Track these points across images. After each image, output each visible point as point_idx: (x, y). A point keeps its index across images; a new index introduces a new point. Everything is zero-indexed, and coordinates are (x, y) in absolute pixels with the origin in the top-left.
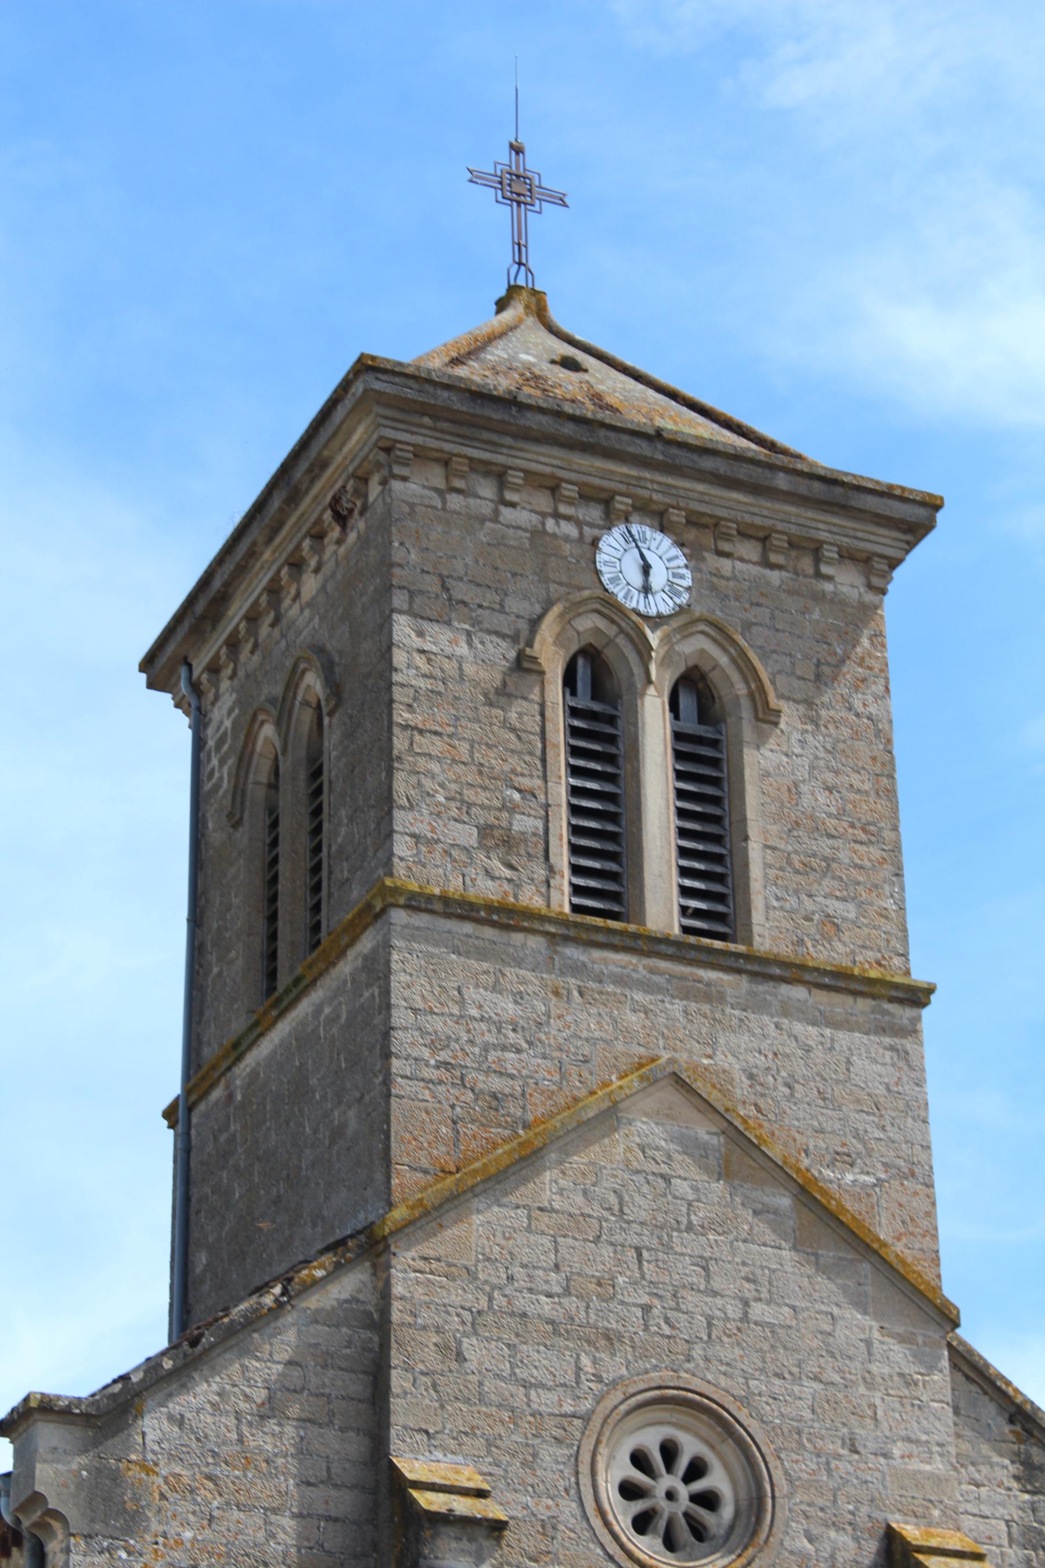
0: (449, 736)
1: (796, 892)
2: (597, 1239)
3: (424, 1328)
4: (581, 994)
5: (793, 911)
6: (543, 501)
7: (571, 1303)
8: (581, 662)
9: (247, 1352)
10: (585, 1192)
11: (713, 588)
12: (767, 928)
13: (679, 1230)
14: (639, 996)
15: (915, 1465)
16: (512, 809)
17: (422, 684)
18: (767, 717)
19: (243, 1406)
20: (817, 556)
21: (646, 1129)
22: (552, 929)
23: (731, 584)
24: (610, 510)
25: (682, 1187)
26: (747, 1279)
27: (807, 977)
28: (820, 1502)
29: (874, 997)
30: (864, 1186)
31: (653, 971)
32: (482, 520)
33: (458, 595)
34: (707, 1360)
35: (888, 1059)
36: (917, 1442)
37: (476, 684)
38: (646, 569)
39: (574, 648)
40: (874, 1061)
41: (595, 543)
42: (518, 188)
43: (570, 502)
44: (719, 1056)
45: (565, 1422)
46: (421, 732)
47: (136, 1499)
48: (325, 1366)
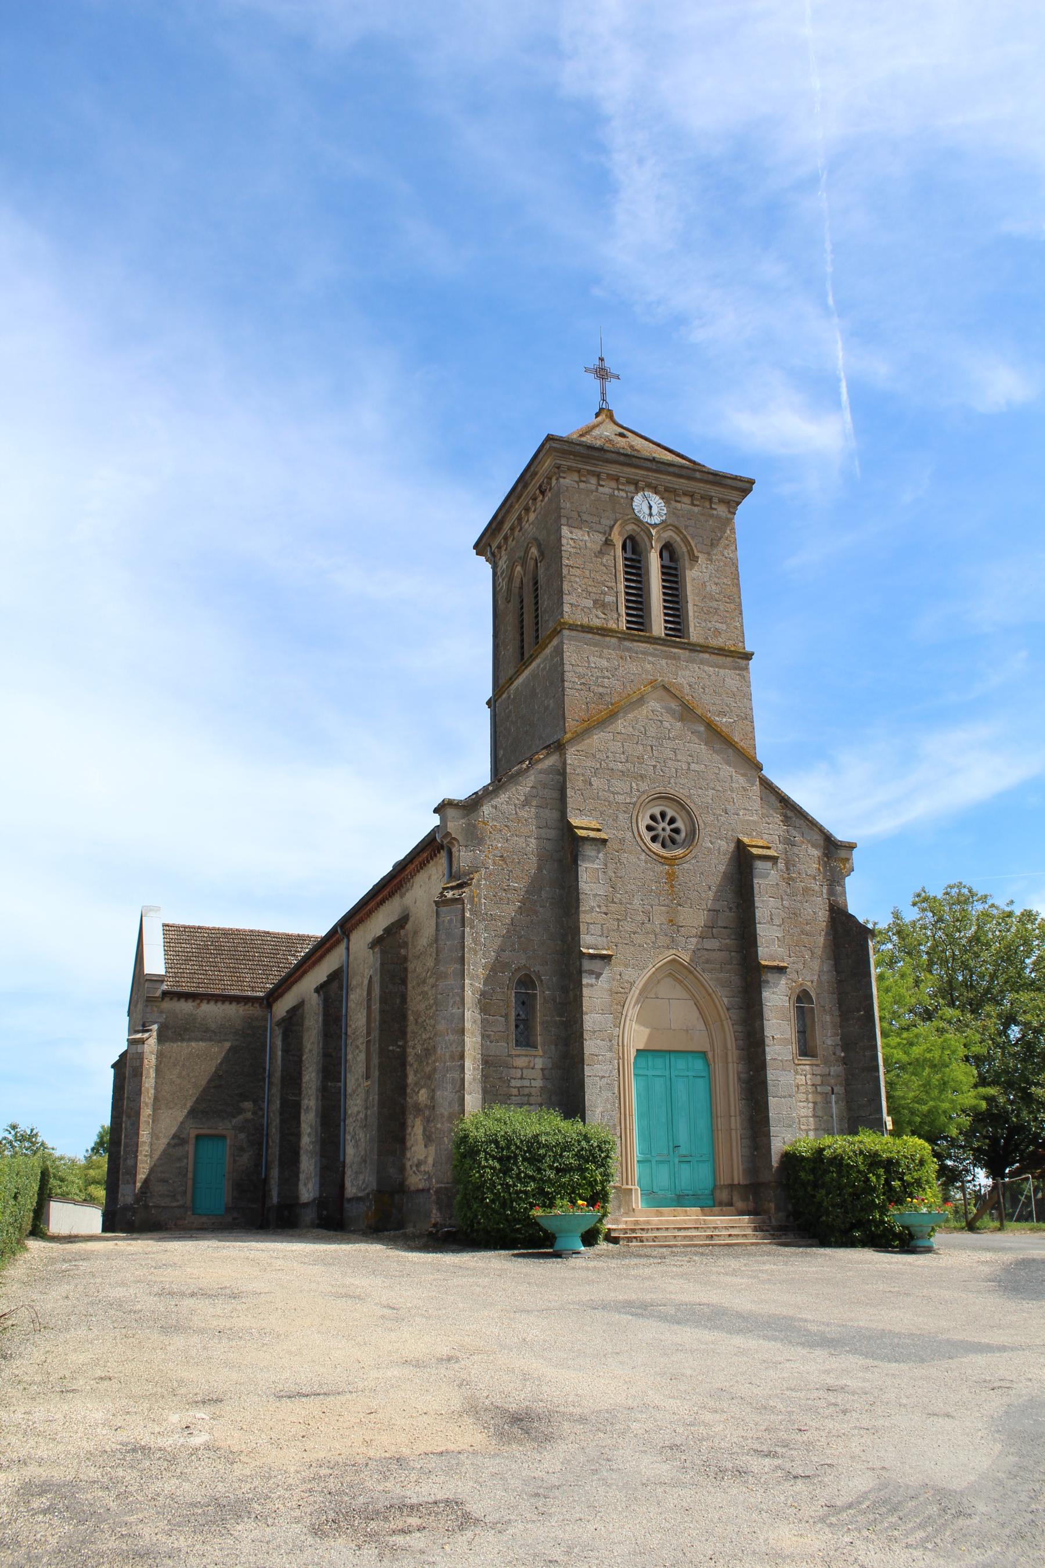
6: (614, 484)
7: (629, 765)
11: (674, 514)
12: (695, 634)
15: (747, 818)
17: (572, 550)
18: (694, 559)
20: (711, 502)
21: (653, 704)
24: (637, 486)
31: (656, 649)
32: (592, 492)
38: (650, 507)
42: (602, 373)
43: (623, 484)
47: (482, 833)
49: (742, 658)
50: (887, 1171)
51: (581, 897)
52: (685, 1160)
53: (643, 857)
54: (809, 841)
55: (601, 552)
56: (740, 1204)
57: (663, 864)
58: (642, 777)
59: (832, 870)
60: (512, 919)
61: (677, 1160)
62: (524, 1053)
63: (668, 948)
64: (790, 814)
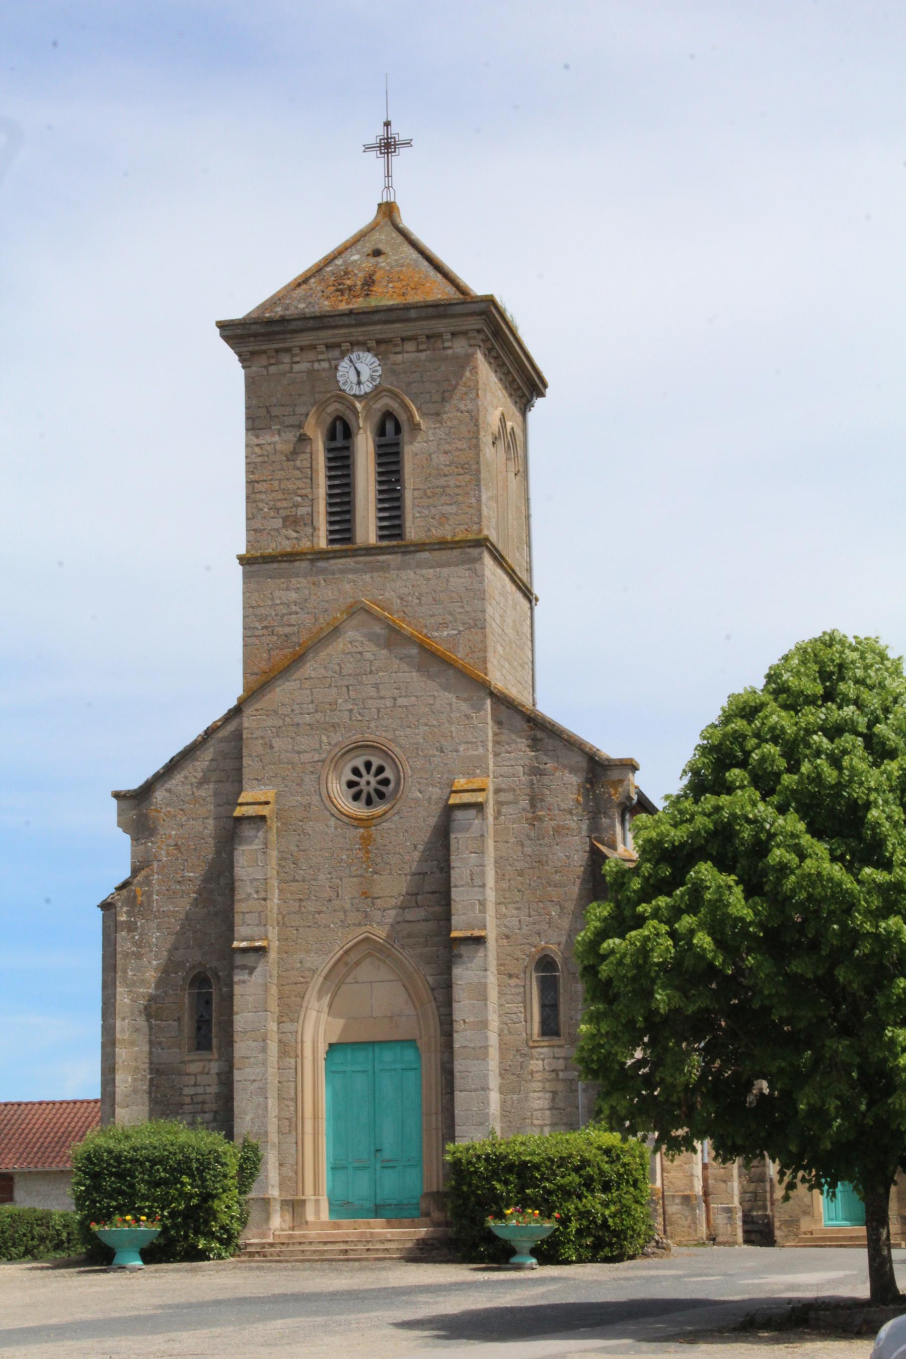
0: (271, 480)
1: (428, 507)
2: (330, 686)
3: (256, 738)
4: (325, 581)
5: (426, 516)
6: (311, 355)
7: (319, 716)
8: (338, 423)
9: (196, 760)
10: (325, 668)
11: (393, 372)
12: (413, 531)
13: (366, 674)
14: (350, 576)
15: (471, 752)
16: (297, 506)
17: (258, 460)
19: (194, 780)
21: (351, 634)
22: (310, 557)
23: (402, 366)
24: (341, 349)
25: (368, 656)
26: (396, 689)
27: (427, 547)
28: (426, 776)
29: (461, 548)
30: (453, 635)
32: (284, 374)
33: (273, 413)
34: (377, 727)
35: (467, 575)
36: (471, 743)
37: (281, 453)
38: (358, 373)
39: (329, 420)
40: (460, 577)
41: (336, 368)
43: (322, 353)
44: (387, 594)
45: (314, 764)
46: (258, 482)
47: (154, 823)
48: (225, 759)
49: (474, 546)
50: (520, 1176)
51: (237, 884)
52: (388, 1165)
53: (332, 822)
54: (565, 767)
55: (294, 454)
56: (436, 1215)
57: (357, 827)
58: (334, 726)
59: (596, 798)
60: (187, 913)
61: (378, 1166)
62: (197, 1057)
63: (360, 925)
64: (539, 734)
